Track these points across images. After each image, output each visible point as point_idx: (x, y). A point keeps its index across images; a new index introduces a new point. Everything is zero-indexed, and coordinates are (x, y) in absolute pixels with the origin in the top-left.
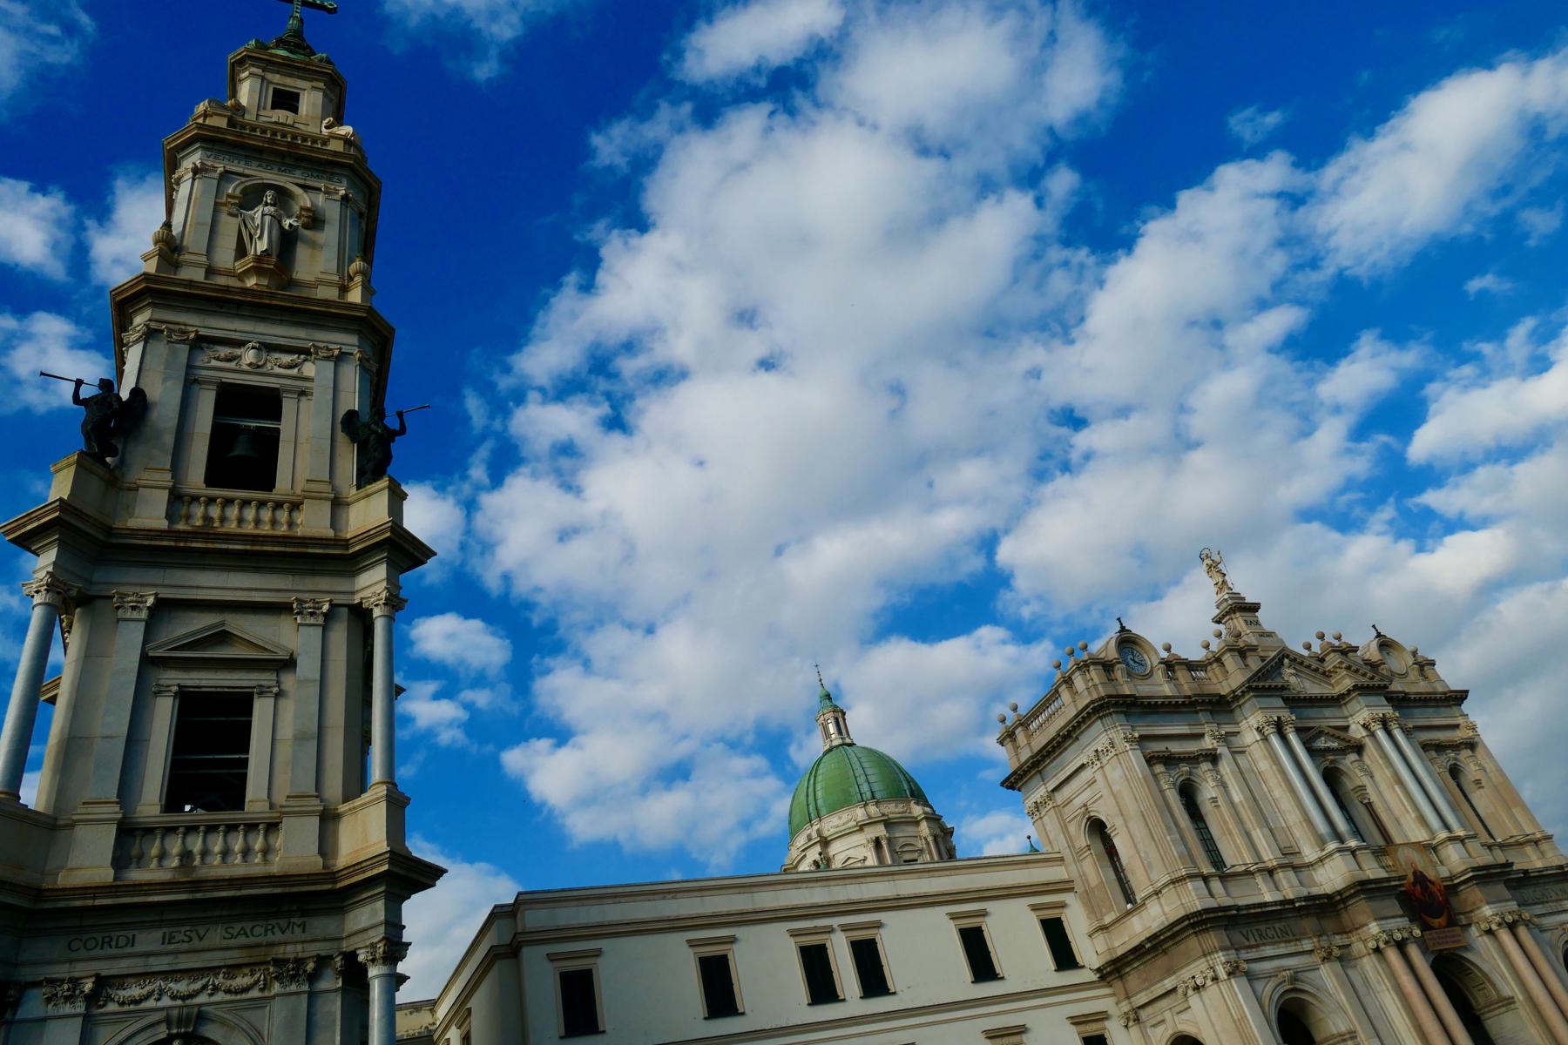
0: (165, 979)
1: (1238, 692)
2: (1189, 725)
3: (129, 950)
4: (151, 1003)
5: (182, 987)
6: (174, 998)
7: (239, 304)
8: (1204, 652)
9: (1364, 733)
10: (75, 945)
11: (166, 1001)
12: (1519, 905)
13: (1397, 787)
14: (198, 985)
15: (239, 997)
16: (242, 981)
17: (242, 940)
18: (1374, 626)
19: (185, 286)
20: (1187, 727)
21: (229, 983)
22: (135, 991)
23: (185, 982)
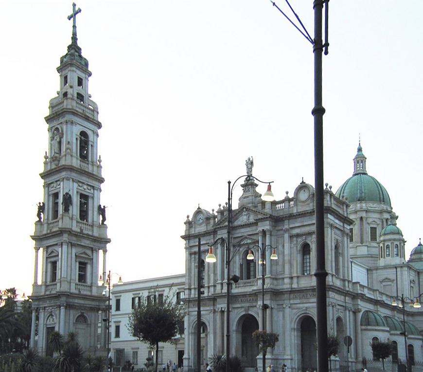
5: (51, 308)
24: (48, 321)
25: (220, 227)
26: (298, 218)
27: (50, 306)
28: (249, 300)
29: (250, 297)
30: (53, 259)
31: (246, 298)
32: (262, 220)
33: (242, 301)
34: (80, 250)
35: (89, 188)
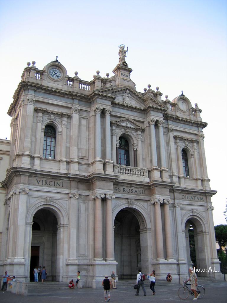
1: (92, 96)
2: (65, 102)
8: (75, 75)
9: (148, 125)
12: (170, 199)
13: (149, 147)
18: (182, 91)
20: (64, 103)
25: (105, 96)
26: (181, 123)
28: (134, 191)
29: (136, 187)
31: (130, 189)
32: (156, 109)
33: (124, 191)
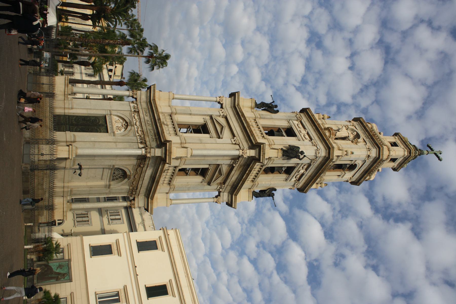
0: (139, 121)
3: (145, 116)
4: (134, 119)
5: (138, 124)
6: (135, 123)
7: (315, 125)
10: (145, 109)
11: (135, 122)
14: (138, 126)
15: (136, 132)
16: (140, 132)
17: (149, 132)
19: (312, 115)
21: (139, 131)
22: (136, 117)
23: (139, 124)
24: (117, 118)
27: (140, 122)
30: (210, 127)
34: (225, 169)
35: (298, 176)
